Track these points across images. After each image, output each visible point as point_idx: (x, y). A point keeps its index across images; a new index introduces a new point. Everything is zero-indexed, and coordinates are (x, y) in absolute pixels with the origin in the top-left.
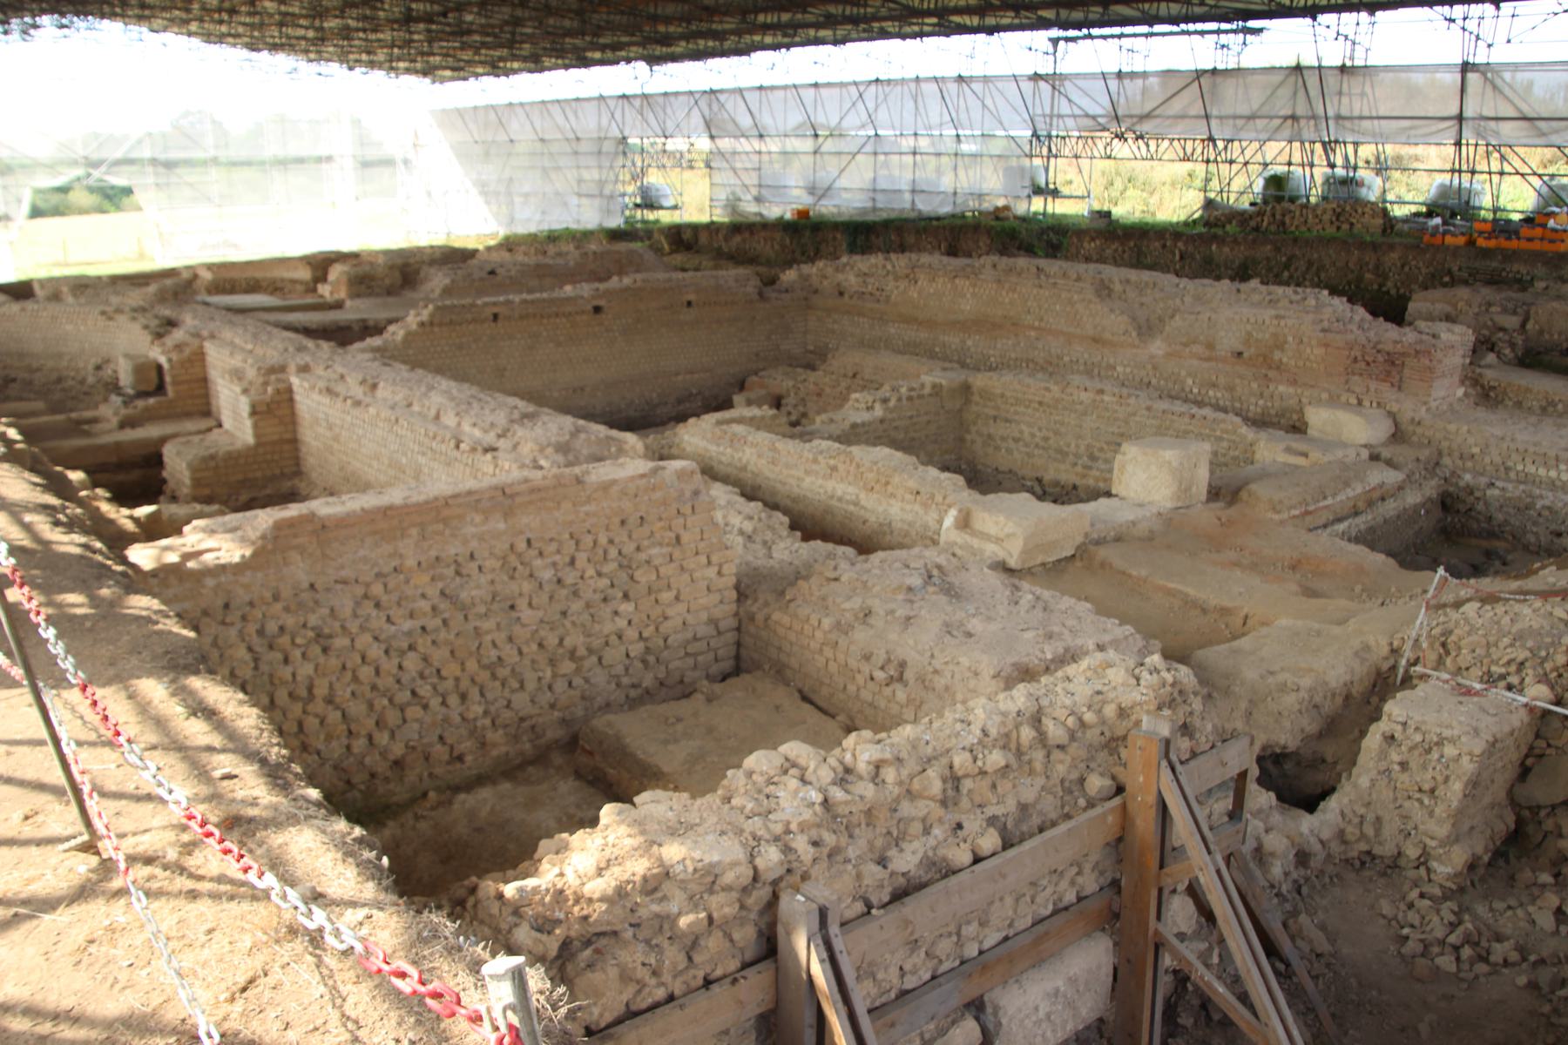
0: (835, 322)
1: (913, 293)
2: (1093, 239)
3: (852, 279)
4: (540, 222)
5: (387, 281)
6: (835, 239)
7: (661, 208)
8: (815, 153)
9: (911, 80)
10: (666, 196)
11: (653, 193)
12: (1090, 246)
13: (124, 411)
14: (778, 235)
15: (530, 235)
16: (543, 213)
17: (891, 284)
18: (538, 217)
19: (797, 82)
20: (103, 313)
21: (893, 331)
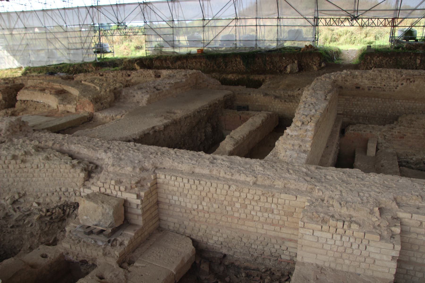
0: (358, 101)
1: (413, 86)
2: (378, 57)
3: (367, 82)
4: (47, 62)
5: (109, 99)
6: (236, 61)
7: (107, 52)
8: (204, 27)
9: (75, 8)
10: (108, 47)
11: (104, 46)
12: (376, 59)
13: (117, 252)
14: (204, 61)
15: (43, 67)
16: (48, 58)
17: (392, 84)
18: (46, 59)
19: (35, 10)
20: (14, 157)
21: (399, 103)
